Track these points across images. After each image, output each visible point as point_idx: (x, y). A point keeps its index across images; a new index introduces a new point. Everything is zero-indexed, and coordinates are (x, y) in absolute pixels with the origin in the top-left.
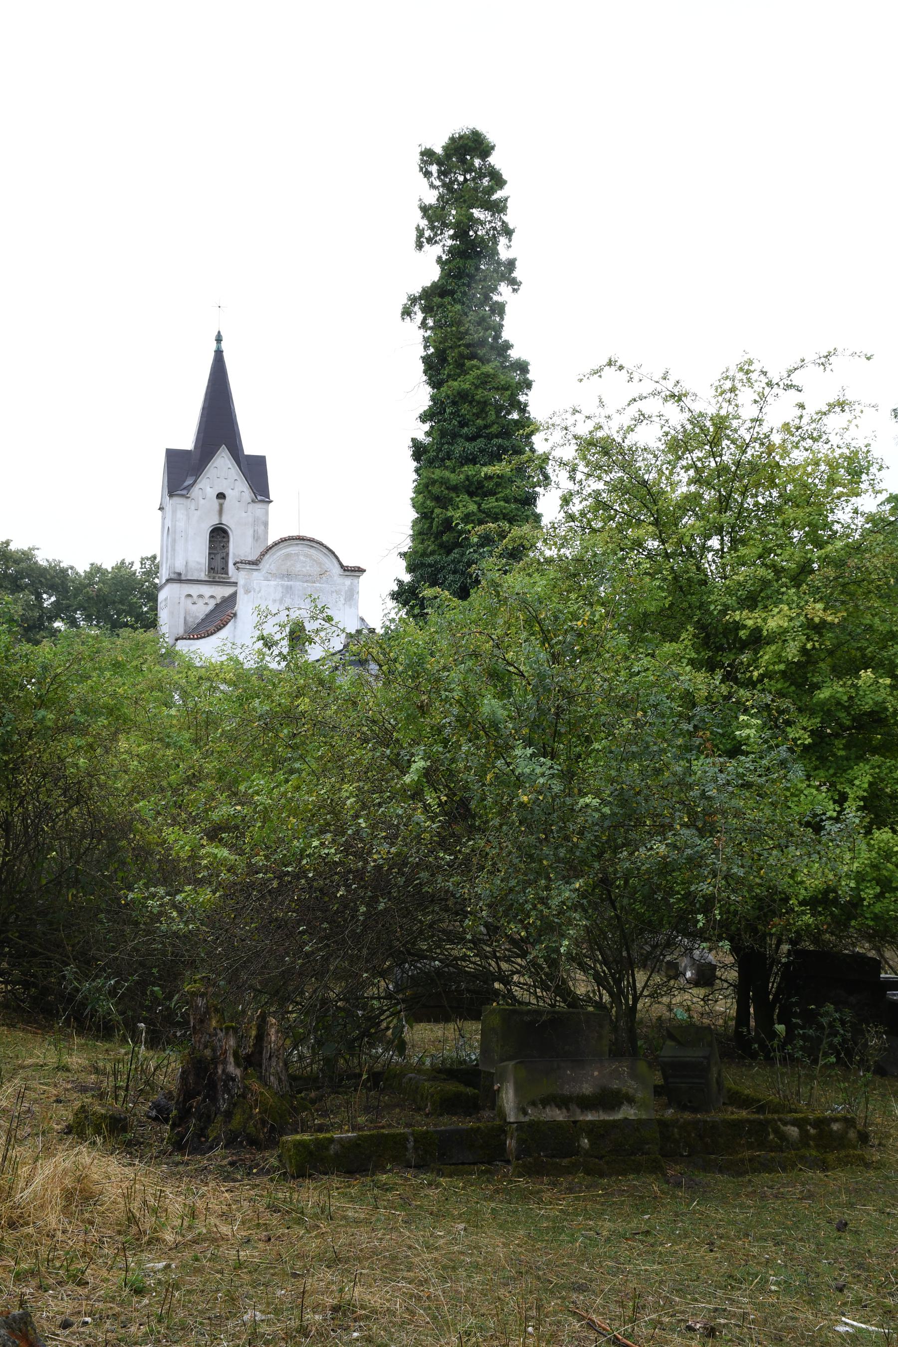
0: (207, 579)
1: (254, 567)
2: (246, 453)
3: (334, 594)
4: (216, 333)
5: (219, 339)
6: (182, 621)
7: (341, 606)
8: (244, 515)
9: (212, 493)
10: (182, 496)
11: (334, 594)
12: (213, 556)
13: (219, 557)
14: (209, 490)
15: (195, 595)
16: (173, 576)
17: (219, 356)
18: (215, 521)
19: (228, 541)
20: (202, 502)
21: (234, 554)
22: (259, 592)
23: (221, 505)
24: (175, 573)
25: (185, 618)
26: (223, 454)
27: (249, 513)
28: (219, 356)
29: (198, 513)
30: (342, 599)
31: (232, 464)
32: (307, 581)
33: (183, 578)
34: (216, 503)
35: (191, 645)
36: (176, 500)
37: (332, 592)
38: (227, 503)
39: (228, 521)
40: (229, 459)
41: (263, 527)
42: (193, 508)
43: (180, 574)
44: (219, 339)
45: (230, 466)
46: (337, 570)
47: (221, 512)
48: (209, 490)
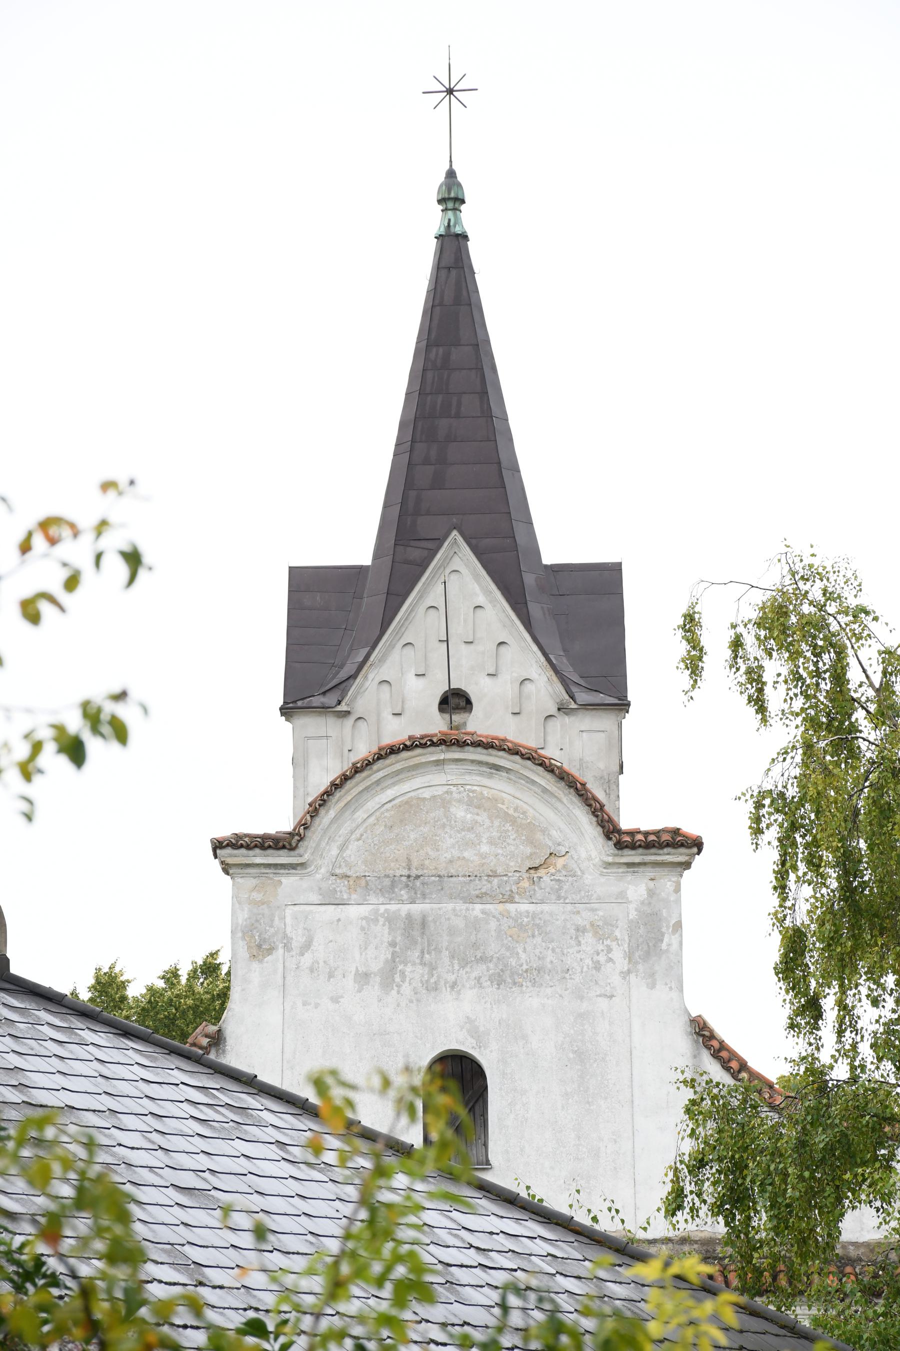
1: (282, 858)
3: (588, 939)
7: (616, 980)
11: (588, 939)
22: (307, 946)
30: (618, 954)
32: (481, 897)
45: (481, 600)
48: (413, 684)
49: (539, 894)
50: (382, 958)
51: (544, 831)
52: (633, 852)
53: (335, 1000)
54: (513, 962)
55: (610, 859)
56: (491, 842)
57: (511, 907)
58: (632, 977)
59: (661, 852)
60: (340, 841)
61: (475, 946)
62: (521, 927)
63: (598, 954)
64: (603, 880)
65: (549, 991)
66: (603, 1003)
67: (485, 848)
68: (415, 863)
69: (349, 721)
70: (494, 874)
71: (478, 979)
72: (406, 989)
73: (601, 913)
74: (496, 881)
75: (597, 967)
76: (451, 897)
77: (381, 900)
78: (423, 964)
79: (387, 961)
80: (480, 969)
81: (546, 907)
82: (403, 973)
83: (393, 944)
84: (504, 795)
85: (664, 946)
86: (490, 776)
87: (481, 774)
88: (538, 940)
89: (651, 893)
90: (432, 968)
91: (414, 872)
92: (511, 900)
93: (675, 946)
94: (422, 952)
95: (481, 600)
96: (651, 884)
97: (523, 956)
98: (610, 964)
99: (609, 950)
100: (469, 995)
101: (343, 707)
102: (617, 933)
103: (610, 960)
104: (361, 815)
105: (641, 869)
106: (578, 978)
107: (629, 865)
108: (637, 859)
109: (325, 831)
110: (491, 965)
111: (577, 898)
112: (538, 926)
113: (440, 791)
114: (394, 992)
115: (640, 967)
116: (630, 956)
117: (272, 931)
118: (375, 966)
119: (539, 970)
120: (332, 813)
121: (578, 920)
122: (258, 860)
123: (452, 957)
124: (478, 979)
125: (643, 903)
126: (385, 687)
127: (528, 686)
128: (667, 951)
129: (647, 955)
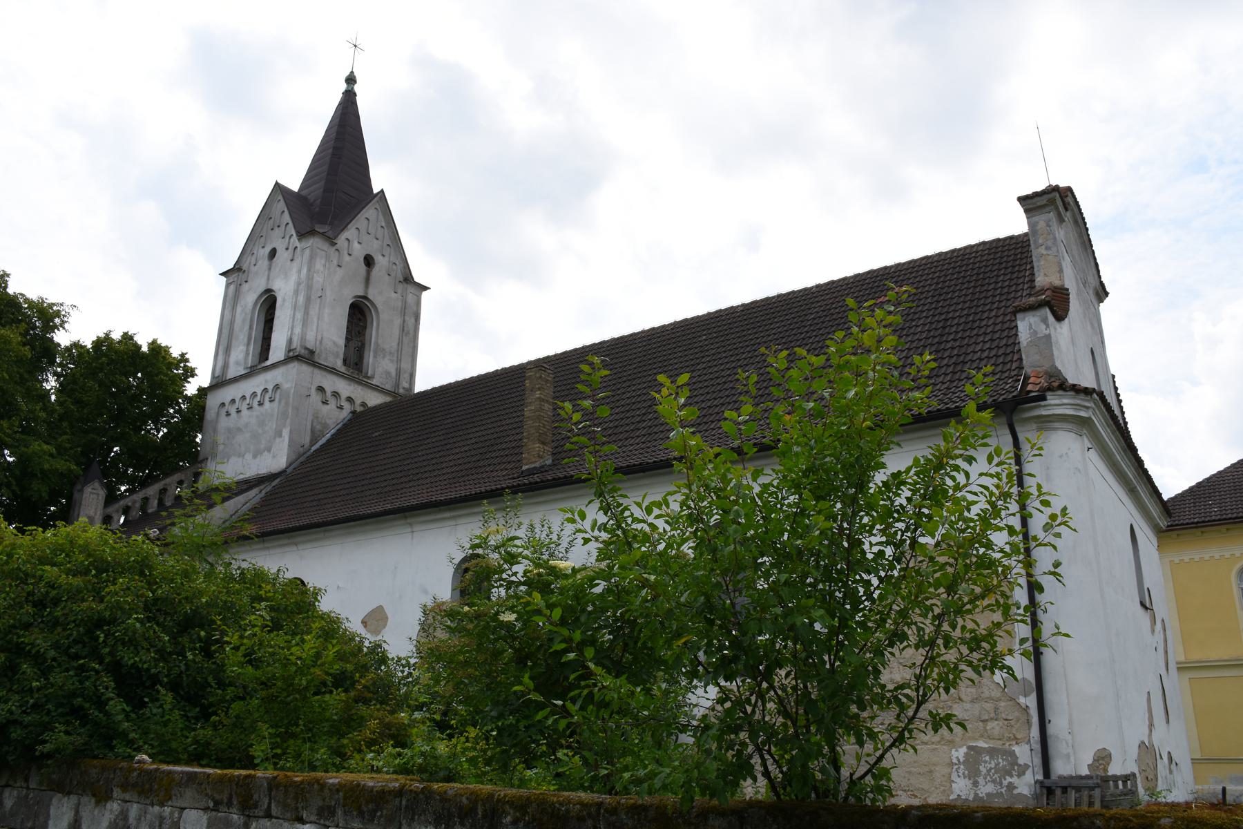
0: (343, 369)
4: (348, 73)
5: (351, 80)
6: (309, 427)
8: (394, 295)
9: (359, 251)
10: (323, 235)
14: (356, 245)
15: (329, 390)
16: (300, 351)
18: (361, 293)
20: (347, 258)
21: (377, 343)
24: (306, 348)
25: (312, 422)
29: (340, 272)
33: (316, 359)
34: (363, 268)
36: (315, 242)
38: (376, 271)
41: (413, 320)
43: (312, 352)
44: (351, 80)
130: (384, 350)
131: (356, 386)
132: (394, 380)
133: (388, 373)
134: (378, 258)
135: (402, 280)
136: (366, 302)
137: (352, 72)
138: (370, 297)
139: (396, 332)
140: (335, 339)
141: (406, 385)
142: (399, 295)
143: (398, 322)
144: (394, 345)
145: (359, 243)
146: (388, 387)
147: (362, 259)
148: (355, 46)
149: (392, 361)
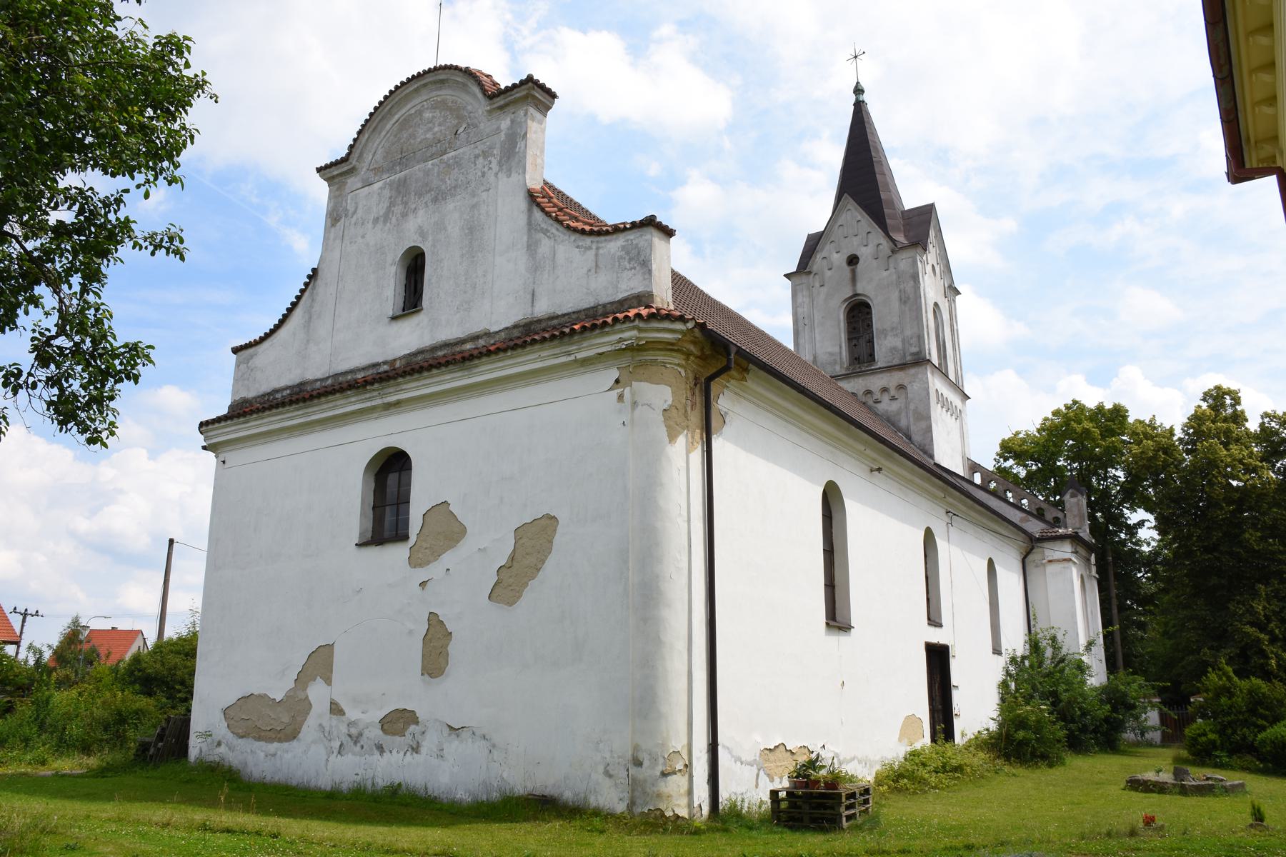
1: (344, 168)
2: (907, 207)
3: (481, 159)
5: (858, 90)
8: (885, 273)
11: (481, 159)
12: (854, 342)
13: (862, 342)
17: (859, 108)
19: (872, 318)
20: (828, 273)
21: (877, 329)
22: (355, 212)
23: (854, 273)
26: (849, 206)
27: (892, 270)
28: (859, 108)
29: (824, 290)
30: (494, 165)
31: (860, 214)
32: (432, 157)
34: (847, 269)
35: (252, 357)
37: (477, 157)
38: (860, 266)
39: (866, 288)
40: (856, 209)
42: (817, 285)
44: (858, 90)
45: (859, 218)
46: (476, 105)
47: (854, 279)
48: (835, 256)
49: (458, 143)
50: (385, 206)
51: (464, 108)
52: (498, 99)
53: (363, 237)
54: (443, 187)
55: (489, 108)
56: (440, 125)
57: (445, 157)
58: (500, 173)
59: (513, 93)
60: (373, 150)
61: (427, 184)
62: (449, 166)
63: (484, 167)
64: (489, 123)
65: (459, 197)
66: (484, 194)
67: (436, 129)
68: (405, 149)
69: (812, 275)
70: (439, 141)
71: (426, 203)
72: (394, 220)
73: (488, 144)
74: (439, 145)
75: (483, 174)
76: (418, 162)
77: (388, 175)
78: (402, 203)
79: (387, 208)
80: (428, 197)
81: (461, 150)
82: (393, 211)
83: (390, 198)
84: (448, 97)
85: (517, 150)
86: (440, 89)
87: (437, 90)
88: (456, 170)
89: (512, 121)
90: (406, 203)
91: (404, 155)
92: (445, 153)
93: (523, 148)
94: (403, 197)
95: (859, 218)
96: (513, 116)
97: (448, 182)
98: (490, 171)
99: (490, 162)
100: (421, 212)
101: (808, 270)
102: (495, 152)
103: (490, 168)
104: (383, 133)
105: (508, 108)
106: (473, 185)
107: (501, 108)
108: (502, 103)
109: (366, 144)
110: (433, 193)
111: (476, 139)
112: (457, 162)
113: (418, 107)
114: (388, 224)
115: (504, 167)
116: (500, 164)
117: (341, 209)
118: (381, 213)
119: (455, 187)
120: (366, 136)
121: (477, 152)
122: (335, 173)
123: (416, 195)
124: (426, 203)
125: (508, 129)
126: (825, 260)
127: (881, 247)
128: (519, 152)
129: (509, 158)
130: (884, 330)
131: (856, 380)
132: (902, 352)
133: (894, 349)
134: (865, 253)
135: (890, 254)
136: (860, 298)
137: (858, 83)
138: (859, 292)
139: (896, 304)
140: (830, 350)
141: (914, 350)
142: (892, 270)
143: (895, 295)
144: (896, 319)
145: (837, 252)
146: (896, 362)
147: (844, 264)
148: (856, 57)
149: (896, 335)
